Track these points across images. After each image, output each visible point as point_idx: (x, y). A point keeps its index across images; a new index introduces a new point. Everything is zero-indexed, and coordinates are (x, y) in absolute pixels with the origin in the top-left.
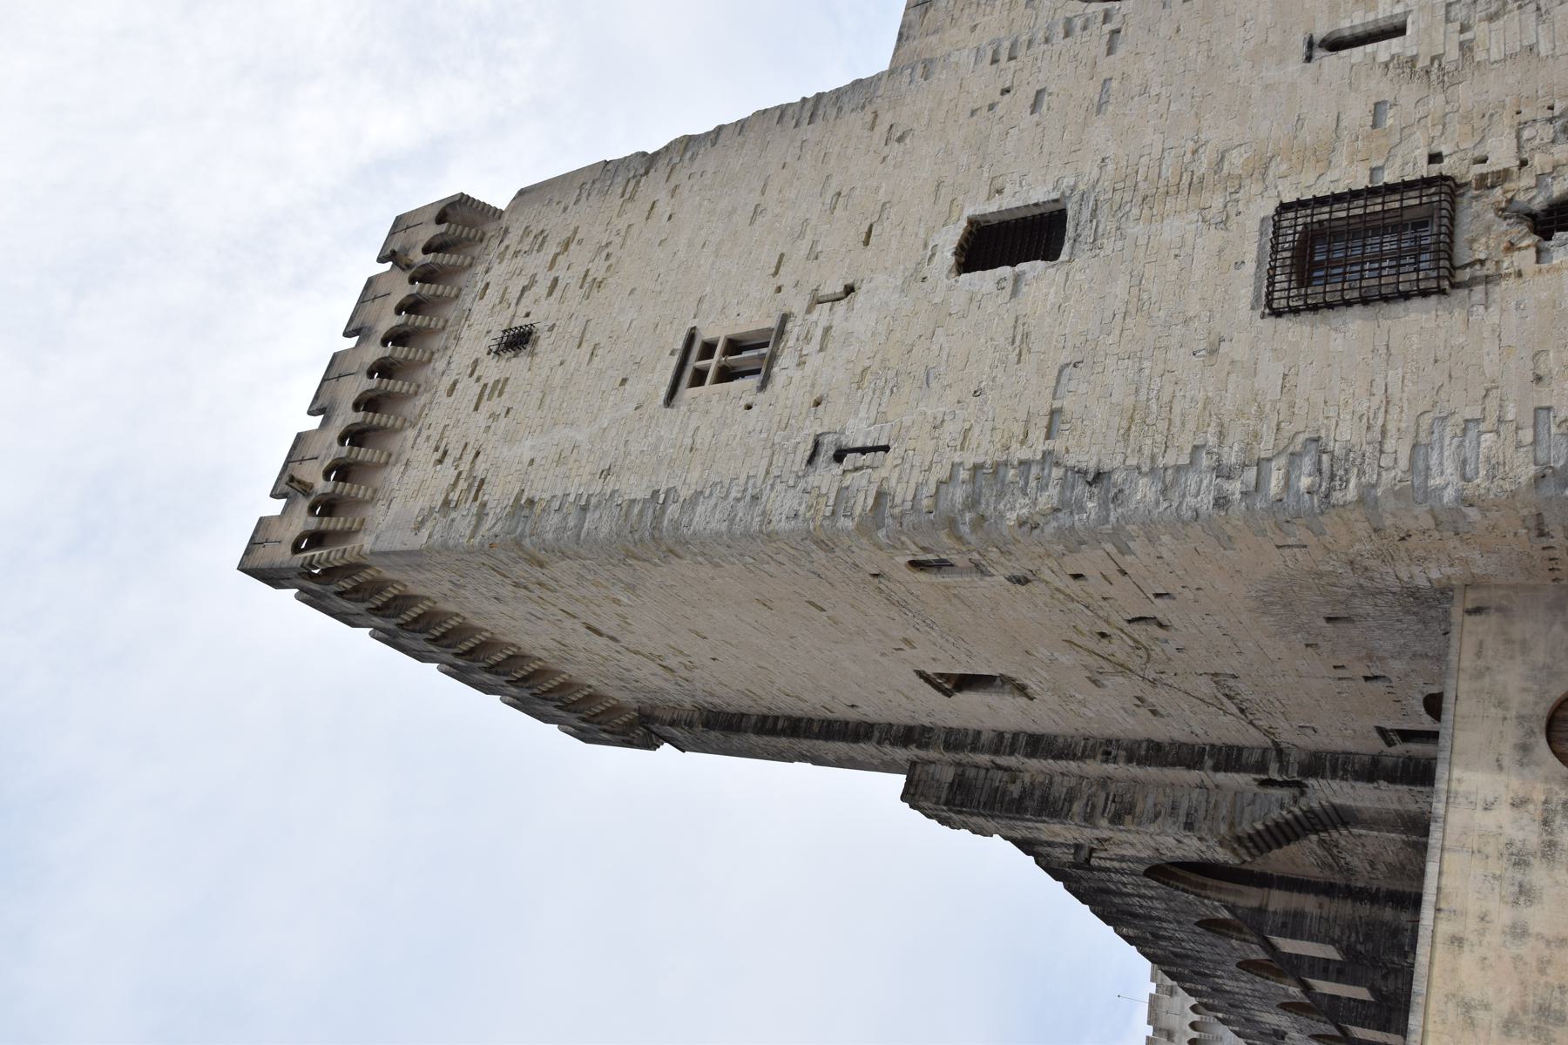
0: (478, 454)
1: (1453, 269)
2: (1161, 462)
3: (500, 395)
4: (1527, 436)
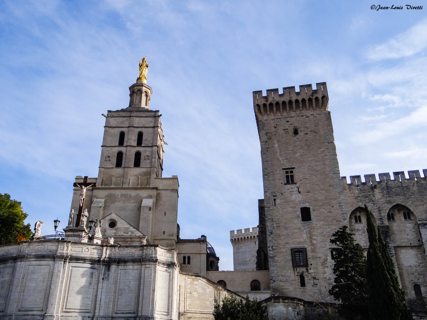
0: (276, 135)
1: (296, 267)
2: (273, 240)
3: (286, 134)
4: (276, 275)
